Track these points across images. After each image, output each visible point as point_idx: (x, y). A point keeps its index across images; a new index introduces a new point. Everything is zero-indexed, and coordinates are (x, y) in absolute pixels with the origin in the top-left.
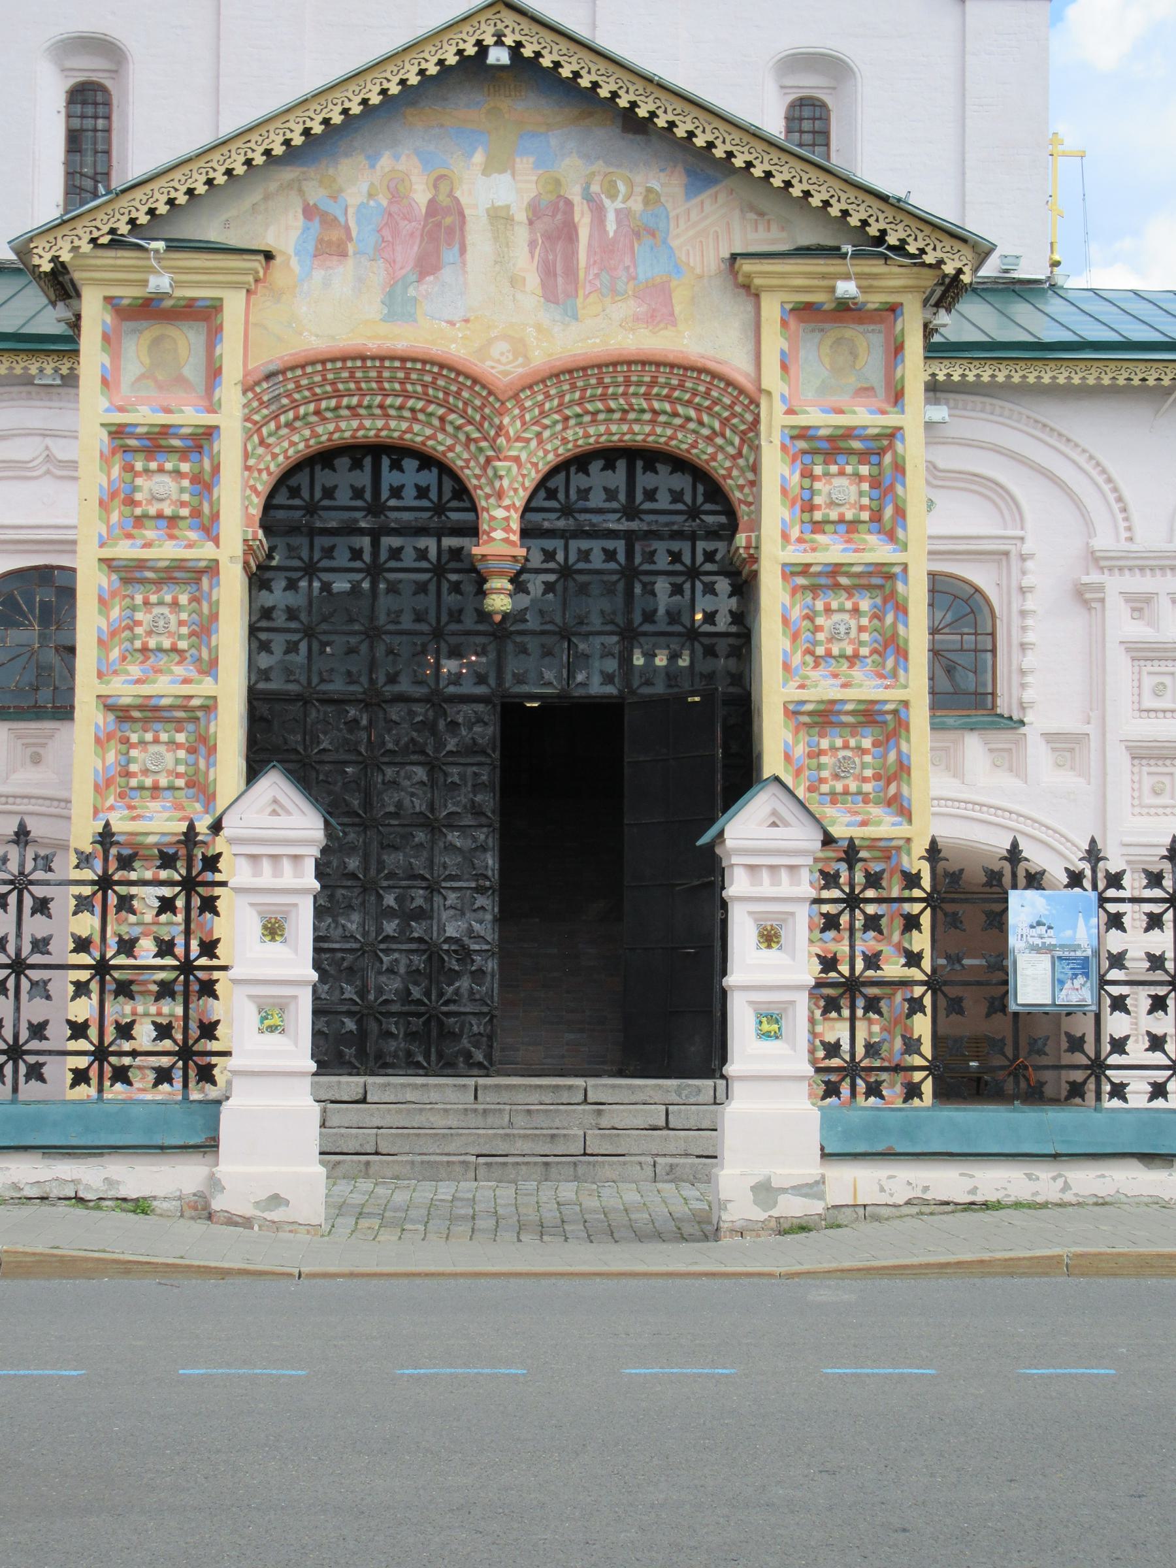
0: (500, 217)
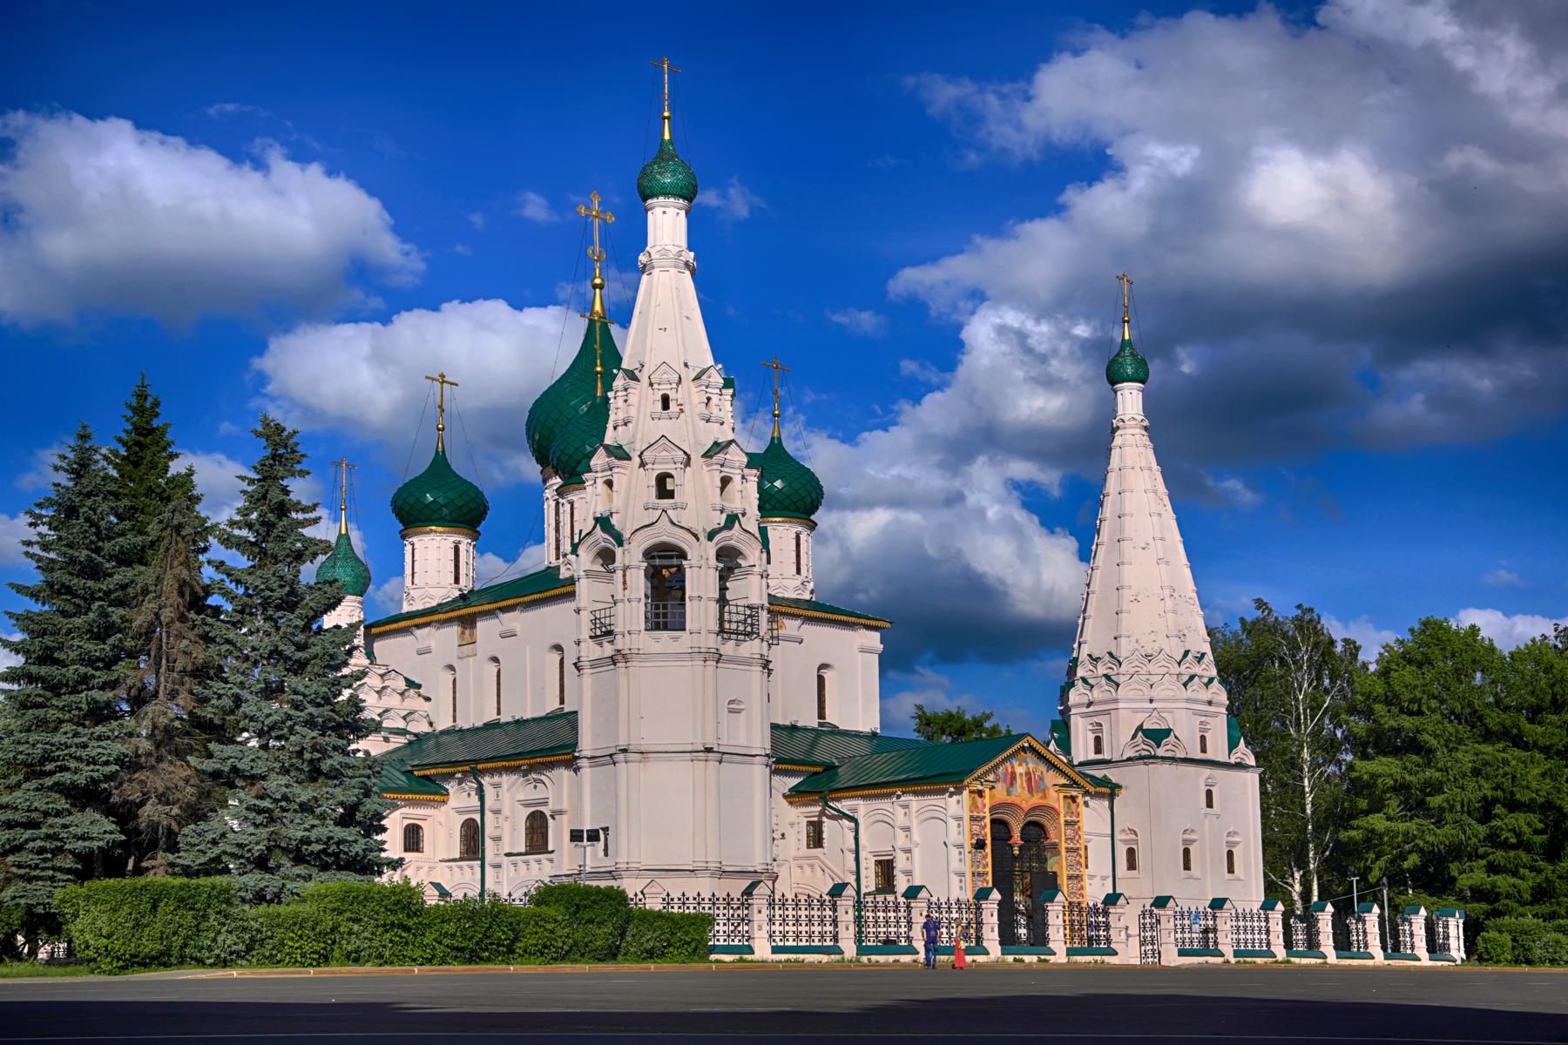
0: (1021, 774)
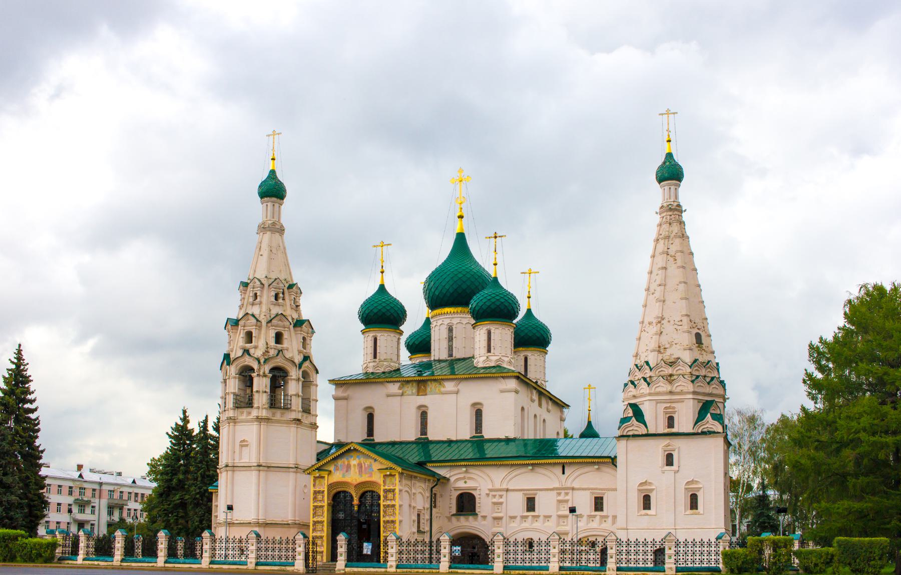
0: (354, 465)
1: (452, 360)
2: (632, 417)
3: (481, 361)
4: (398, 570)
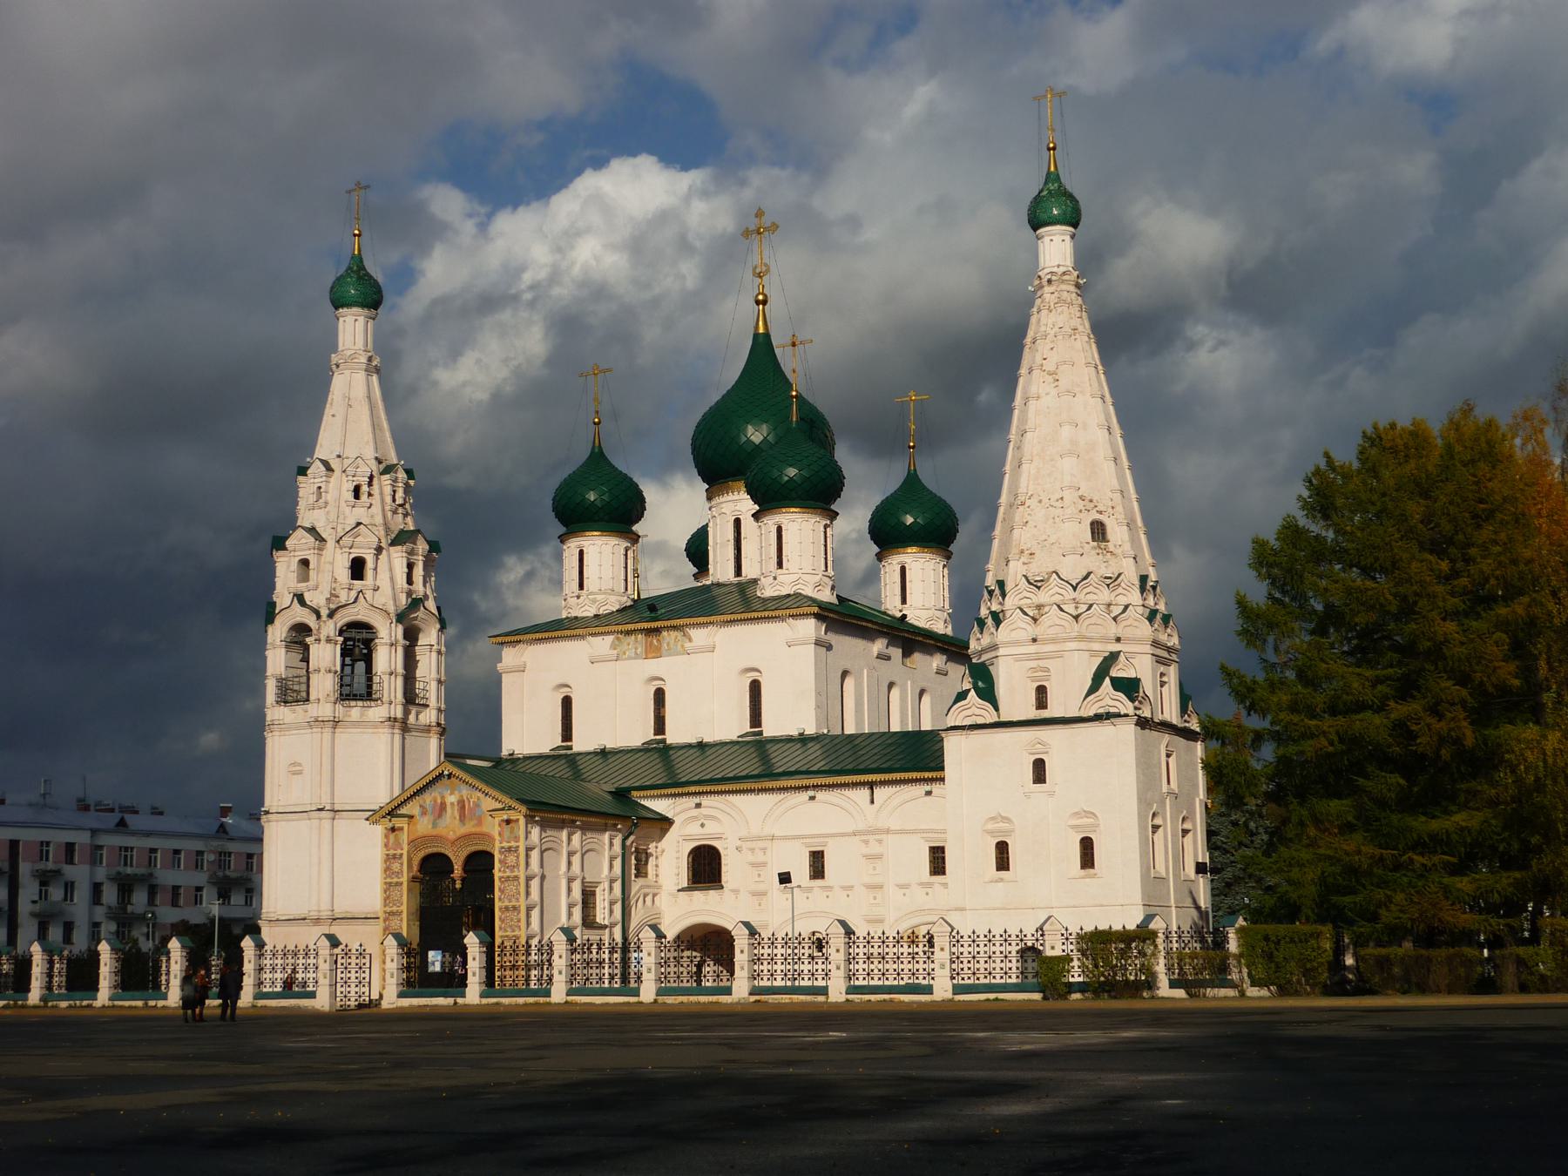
0: (452, 804)
1: (739, 584)
2: (969, 690)
3: (768, 590)
4: (485, 1001)
